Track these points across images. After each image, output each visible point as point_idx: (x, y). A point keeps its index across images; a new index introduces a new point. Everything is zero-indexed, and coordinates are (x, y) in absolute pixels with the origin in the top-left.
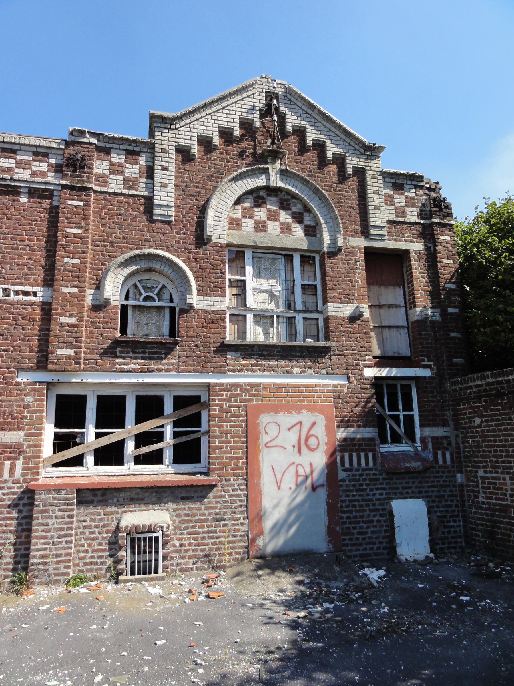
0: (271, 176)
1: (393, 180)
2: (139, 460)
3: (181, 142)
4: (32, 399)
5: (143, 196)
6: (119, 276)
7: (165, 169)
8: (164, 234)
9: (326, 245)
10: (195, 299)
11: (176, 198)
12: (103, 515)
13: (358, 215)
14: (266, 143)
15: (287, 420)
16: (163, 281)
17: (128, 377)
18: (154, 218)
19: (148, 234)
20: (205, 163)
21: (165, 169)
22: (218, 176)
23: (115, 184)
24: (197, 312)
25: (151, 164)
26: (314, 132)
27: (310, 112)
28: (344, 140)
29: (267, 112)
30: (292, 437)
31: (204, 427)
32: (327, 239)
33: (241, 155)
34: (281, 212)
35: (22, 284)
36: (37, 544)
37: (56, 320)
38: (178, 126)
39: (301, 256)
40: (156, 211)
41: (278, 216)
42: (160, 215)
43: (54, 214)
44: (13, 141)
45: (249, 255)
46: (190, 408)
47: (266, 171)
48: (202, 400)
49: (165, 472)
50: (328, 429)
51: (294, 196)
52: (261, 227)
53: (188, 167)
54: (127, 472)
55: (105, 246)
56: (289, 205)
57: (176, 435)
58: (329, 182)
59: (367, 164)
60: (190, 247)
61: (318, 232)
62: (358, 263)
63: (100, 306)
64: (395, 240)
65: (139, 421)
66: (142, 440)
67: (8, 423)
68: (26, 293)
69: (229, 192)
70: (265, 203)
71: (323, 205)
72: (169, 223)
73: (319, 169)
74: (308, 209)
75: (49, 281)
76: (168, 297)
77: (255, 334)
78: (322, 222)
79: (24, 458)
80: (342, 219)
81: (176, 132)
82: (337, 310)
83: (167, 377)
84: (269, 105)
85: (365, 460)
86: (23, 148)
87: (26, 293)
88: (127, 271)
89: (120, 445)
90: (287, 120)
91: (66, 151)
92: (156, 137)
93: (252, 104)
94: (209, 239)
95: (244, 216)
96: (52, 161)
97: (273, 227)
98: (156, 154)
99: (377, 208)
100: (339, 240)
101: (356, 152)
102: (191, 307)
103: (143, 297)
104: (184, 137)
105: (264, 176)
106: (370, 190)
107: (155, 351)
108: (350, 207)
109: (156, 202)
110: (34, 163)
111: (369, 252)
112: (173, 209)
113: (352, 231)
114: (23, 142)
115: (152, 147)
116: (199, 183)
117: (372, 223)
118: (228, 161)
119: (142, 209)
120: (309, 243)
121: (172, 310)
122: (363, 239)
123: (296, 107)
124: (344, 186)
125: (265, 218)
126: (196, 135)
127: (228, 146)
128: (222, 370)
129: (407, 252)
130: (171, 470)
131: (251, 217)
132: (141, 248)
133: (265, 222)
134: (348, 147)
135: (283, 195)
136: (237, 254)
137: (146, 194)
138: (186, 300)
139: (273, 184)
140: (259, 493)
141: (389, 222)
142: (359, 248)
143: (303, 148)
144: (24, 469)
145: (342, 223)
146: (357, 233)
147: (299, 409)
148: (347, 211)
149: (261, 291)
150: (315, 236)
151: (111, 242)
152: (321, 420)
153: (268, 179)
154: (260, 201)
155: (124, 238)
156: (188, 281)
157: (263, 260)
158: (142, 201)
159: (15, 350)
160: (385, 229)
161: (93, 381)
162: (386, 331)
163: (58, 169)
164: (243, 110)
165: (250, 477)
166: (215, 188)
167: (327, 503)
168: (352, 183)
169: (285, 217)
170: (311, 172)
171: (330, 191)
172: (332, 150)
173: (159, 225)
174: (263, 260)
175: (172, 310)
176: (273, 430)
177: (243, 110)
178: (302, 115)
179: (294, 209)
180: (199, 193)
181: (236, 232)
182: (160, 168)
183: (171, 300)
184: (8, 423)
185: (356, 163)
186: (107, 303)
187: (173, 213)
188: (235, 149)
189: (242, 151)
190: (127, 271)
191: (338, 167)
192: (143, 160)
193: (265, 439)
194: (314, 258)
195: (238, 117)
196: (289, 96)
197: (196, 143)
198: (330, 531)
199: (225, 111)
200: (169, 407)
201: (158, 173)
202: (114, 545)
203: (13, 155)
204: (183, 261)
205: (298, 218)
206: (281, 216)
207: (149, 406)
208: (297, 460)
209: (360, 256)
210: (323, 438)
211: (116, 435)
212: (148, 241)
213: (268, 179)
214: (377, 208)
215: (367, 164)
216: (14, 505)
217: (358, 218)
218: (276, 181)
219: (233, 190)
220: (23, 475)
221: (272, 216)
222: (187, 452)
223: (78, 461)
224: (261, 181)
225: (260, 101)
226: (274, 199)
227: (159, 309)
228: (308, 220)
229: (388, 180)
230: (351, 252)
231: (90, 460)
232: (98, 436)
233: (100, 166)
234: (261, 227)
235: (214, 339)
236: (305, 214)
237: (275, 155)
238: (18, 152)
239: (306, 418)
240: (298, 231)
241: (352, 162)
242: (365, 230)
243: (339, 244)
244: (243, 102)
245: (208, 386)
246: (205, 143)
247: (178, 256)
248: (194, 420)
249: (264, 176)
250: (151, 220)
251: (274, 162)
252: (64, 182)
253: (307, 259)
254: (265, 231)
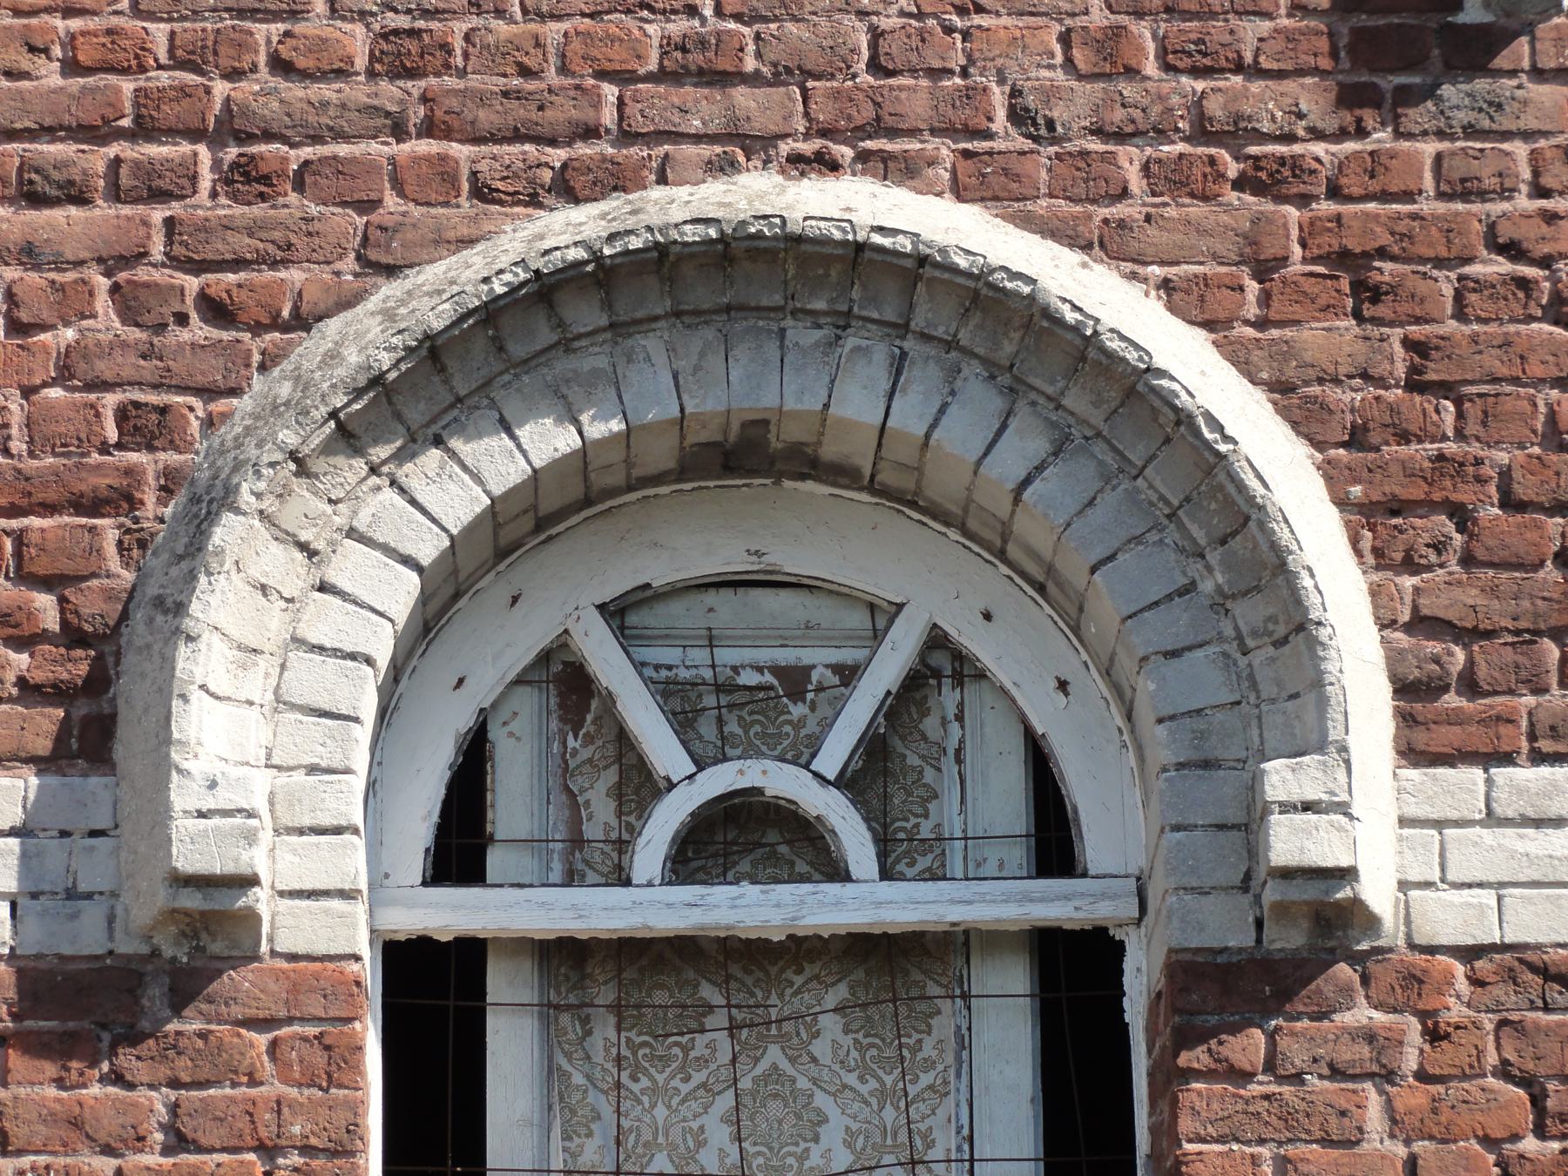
6: (354, 567)
10: (1369, 815)
16: (935, 587)
24: (1412, 987)
55: (156, 188)
60: (1265, 103)
76: (1003, 801)
88: (459, 484)
102: (1327, 914)
103: (667, 819)
121: (1074, 969)
132: (617, 180)
138: (1248, 823)
151: (232, 127)
155: (398, 57)
156: (1270, 571)
175: (1074, 969)
183: (1054, 845)
186: (211, 923)
190: (459, 484)
204: (1190, 302)
227: (890, 965)
247: (1110, 245)
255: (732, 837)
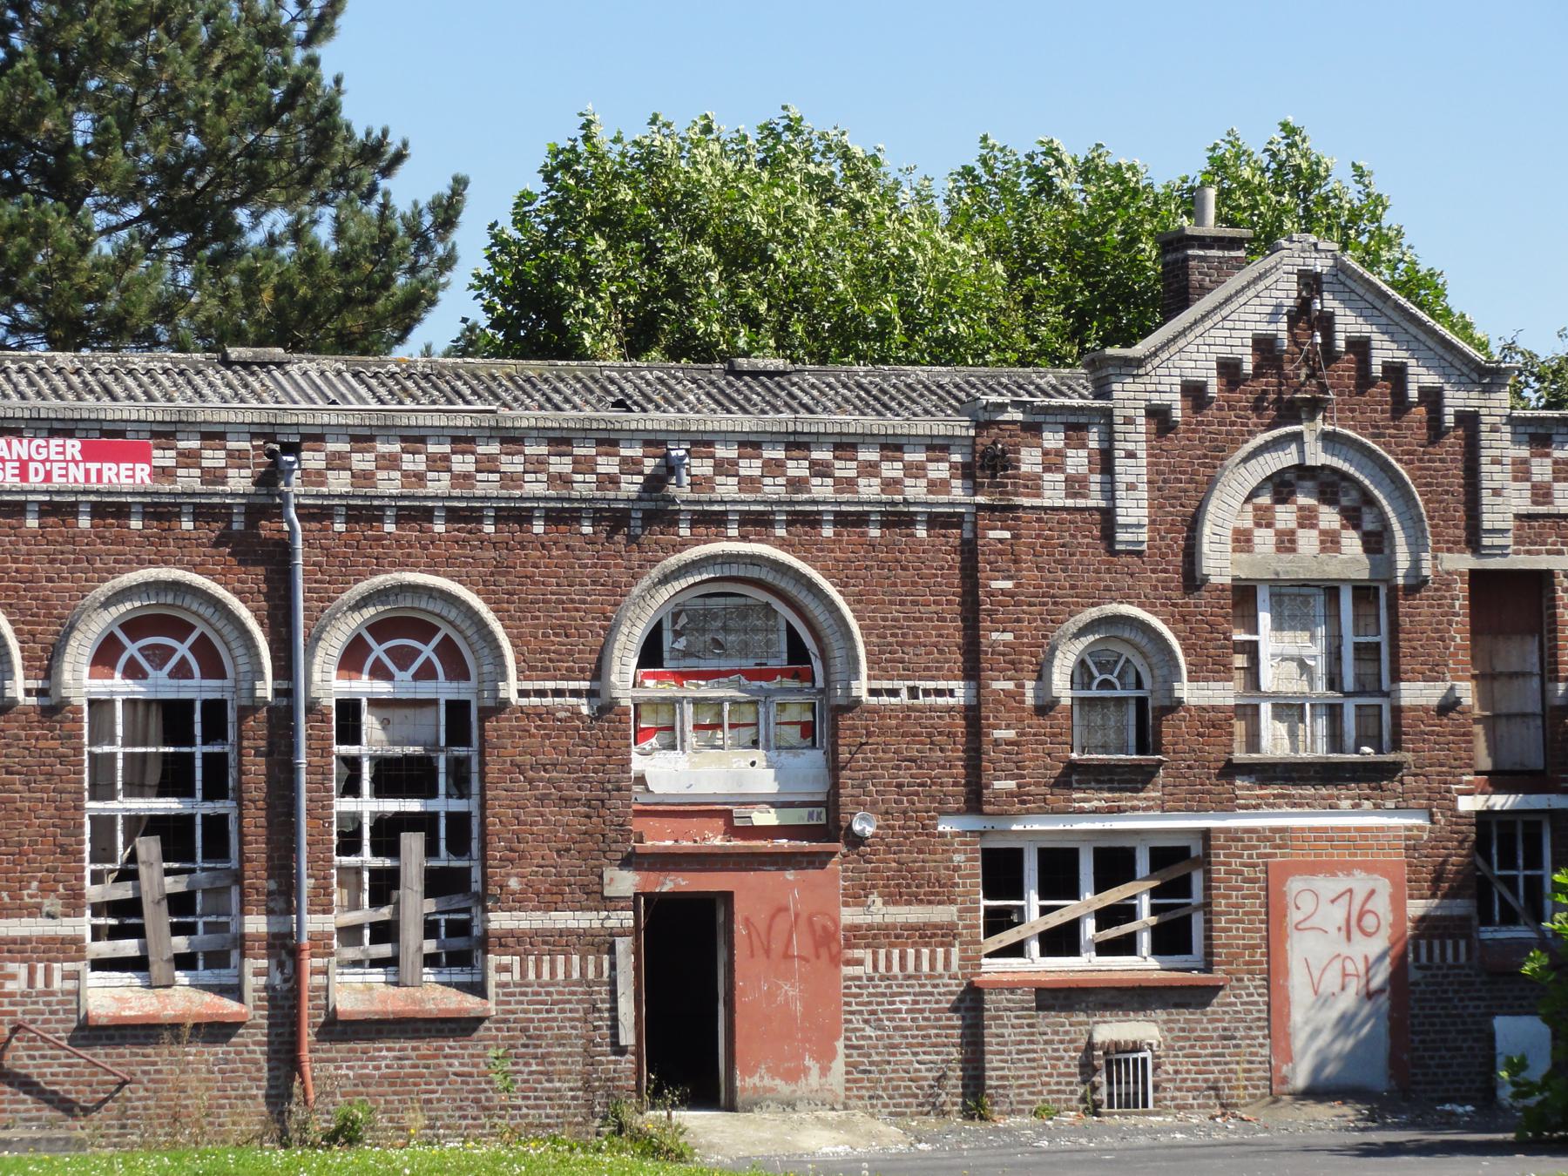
0: (1306, 447)
1: (1531, 430)
2: (1104, 949)
3: (1156, 399)
4: (963, 857)
5: (1097, 509)
6: (1069, 655)
7: (1131, 455)
8: (1132, 575)
9: (1400, 573)
10: (1186, 691)
11: (1150, 506)
12: (1071, 1026)
13: (1461, 507)
14: (1298, 376)
15: (1329, 886)
16: (1127, 652)
17: (1089, 820)
18: (1118, 547)
19: (1107, 576)
20: (1194, 431)
21: (1131, 455)
22: (1217, 454)
23: (1054, 494)
24: (1188, 710)
25: (1106, 445)
26: (1387, 345)
27: (1378, 304)
28: (1442, 358)
29: (1301, 315)
30: (1338, 914)
31: (1197, 896)
32: (1403, 561)
33: (1257, 408)
34: (1324, 509)
35: (933, 678)
36: (992, 1061)
37: (988, 735)
38: (1149, 367)
39: (1355, 589)
40: (1121, 536)
41: (1316, 517)
42: (1127, 542)
43: (969, 552)
44: (899, 431)
45: (1263, 595)
46: (1177, 864)
47: (1298, 438)
48: (1193, 854)
49: (1143, 965)
50: (1398, 905)
51: (1345, 476)
52: (1286, 542)
53: (1166, 444)
54: (1085, 965)
55: (1045, 604)
56: (1336, 493)
57: (1155, 910)
58: (1410, 444)
59: (1482, 403)
60: (1174, 594)
61: (1386, 543)
62: (1457, 603)
63: (1045, 707)
64: (1528, 552)
65: (1100, 887)
66: (1106, 917)
67: (936, 894)
68: (939, 693)
69: (1234, 484)
70: (1293, 493)
71: (1397, 494)
72: (1139, 554)
73: (1393, 419)
74: (1369, 500)
75: (972, 673)
76: (1132, 679)
77: (1275, 741)
78: (1396, 526)
79: (961, 944)
80: (1431, 518)
81: (1146, 379)
82: (1416, 694)
83: (1146, 820)
84: (1304, 306)
85: (1453, 952)
86: (912, 440)
87: (939, 693)
89: (1073, 926)
90: (1338, 328)
91: (979, 440)
92: (1115, 395)
93: (1274, 302)
94: (1205, 579)
95: (1258, 525)
96: (956, 458)
97: (1308, 541)
98: (1117, 428)
99: (1496, 492)
100: (1424, 564)
101: (1463, 379)
102: (1180, 701)
103: (1096, 682)
104: (1160, 388)
105: (1294, 447)
106: (1486, 455)
107: (1132, 779)
108: (1447, 492)
109: (1120, 520)
110: (930, 466)
111: (1476, 576)
112: (1145, 530)
113: (1448, 542)
114: (913, 432)
115: (1108, 414)
116: (1185, 473)
117: (1486, 525)
118: (1233, 424)
119: (1096, 533)
120: (1373, 569)
121: (1141, 703)
122: (1468, 556)
123: (1354, 297)
124: (1437, 449)
125: (1293, 525)
126: (1178, 380)
127: (1232, 391)
128: (1227, 806)
129: (1549, 574)
130: (1153, 963)
131: (1269, 525)
132: (1098, 604)
133: (1293, 532)
134: (1448, 371)
135: (1324, 477)
136: (1243, 596)
137: (1103, 504)
138: (1172, 690)
139: (1310, 462)
140: (1287, 1001)
141: (1518, 517)
142: (1461, 574)
143: (1364, 380)
144: (962, 959)
145: (1432, 526)
146: (1456, 543)
147: (1348, 868)
148: (1441, 502)
149: (1286, 656)
150: (1381, 551)
151: (1053, 596)
152: (1383, 886)
153: (1301, 452)
154: (1286, 490)
155: (1073, 587)
156: (1175, 659)
157: (1286, 599)
158: (1097, 517)
159: (934, 783)
160: (1510, 534)
161: (1035, 828)
162: (1502, 727)
163: (967, 472)
164: (1257, 317)
165: (1273, 976)
166: (1212, 482)
167: (1390, 1018)
168: (1453, 443)
169: (1329, 518)
170: (1377, 427)
171: (1412, 462)
172: (1421, 377)
173: (1124, 559)
174: (1286, 599)
175: (1141, 703)
176: (1307, 902)
177: (1257, 317)
178: (1366, 312)
179: (1345, 501)
180: (1185, 491)
181: (1244, 555)
182: (1123, 454)
183: (1139, 685)
184: (936, 894)
185: (1461, 402)
186: (1056, 701)
187: (1144, 537)
188: (1244, 397)
189: (1257, 400)
191: (1428, 413)
192: (1093, 440)
193: (1294, 916)
194: (1377, 589)
195: (1250, 334)
196: (1342, 277)
197: (1179, 396)
198: (1394, 1060)
199: (1228, 324)
200: (1143, 864)
201: (1121, 464)
202: (1087, 1069)
203: (898, 454)
204: (1165, 622)
205: (1352, 518)
206: (1321, 517)
207: (1114, 864)
208: (1345, 950)
209: (1461, 588)
210: (1387, 916)
211: (1069, 910)
212: (1108, 589)
213: (1301, 452)
214: (1496, 492)
215: (1482, 403)
216: (954, 1009)
217: (1460, 514)
218: (1317, 456)
219: (1241, 480)
220: (961, 967)
221: (1307, 519)
222: (1171, 939)
223: (1017, 950)
224: (1289, 457)
225: (1286, 292)
226: (1309, 484)
227: (1120, 701)
228: (1369, 524)
229: (1521, 429)
230: (1445, 581)
231: (1034, 947)
232: (1045, 911)
233: (1029, 460)
234: (1286, 542)
235: (1215, 753)
236: (1364, 509)
237: (1314, 407)
238: (906, 448)
239: (1360, 883)
240: (1352, 543)
241: (1456, 400)
242: (1473, 542)
243: (1425, 572)
244: (1257, 301)
245: (1206, 834)
246: (1194, 392)
247: (1155, 614)
248: (1181, 887)
249: (1294, 447)
250: (1115, 553)
251: (1312, 418)
252: (980, 499)
253: (1364, 593)
254: (1294, 550)
255: (1105, 684)
